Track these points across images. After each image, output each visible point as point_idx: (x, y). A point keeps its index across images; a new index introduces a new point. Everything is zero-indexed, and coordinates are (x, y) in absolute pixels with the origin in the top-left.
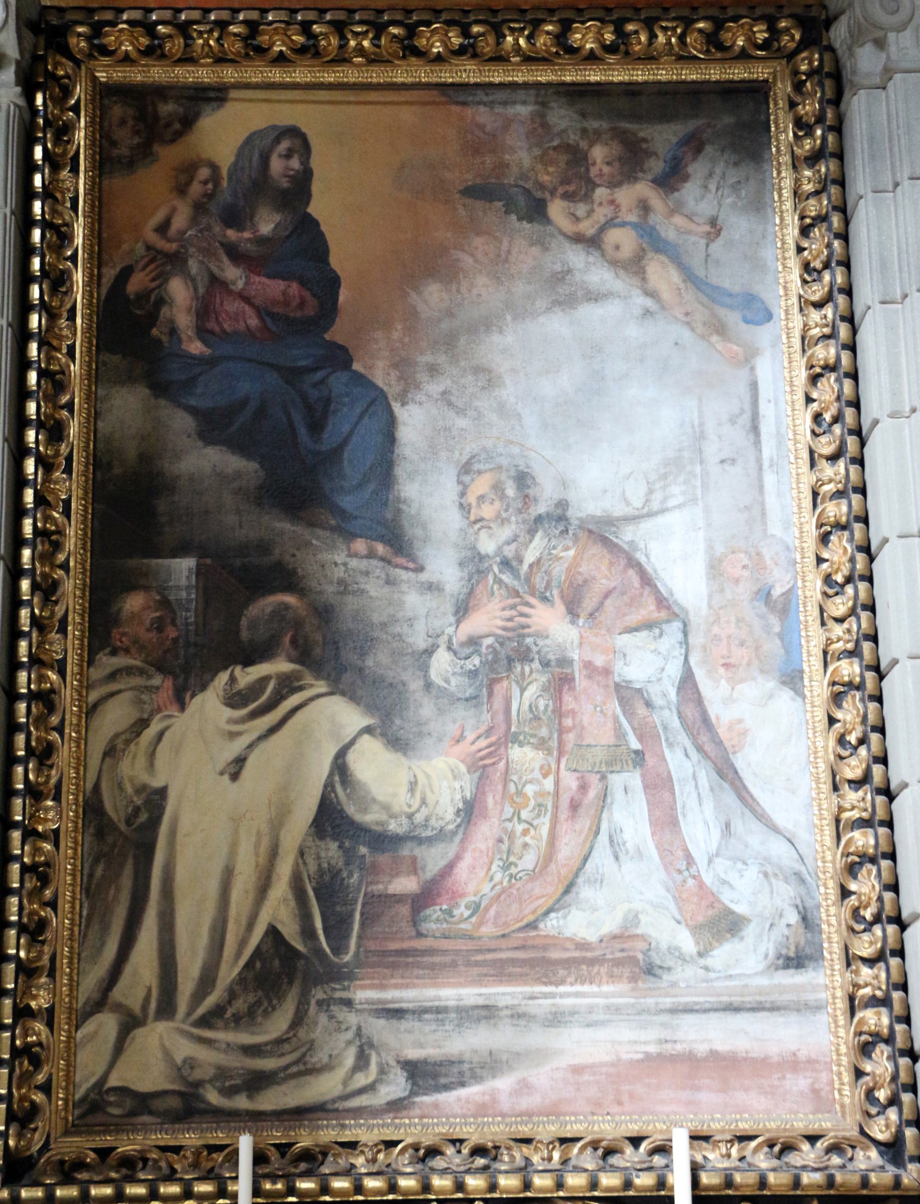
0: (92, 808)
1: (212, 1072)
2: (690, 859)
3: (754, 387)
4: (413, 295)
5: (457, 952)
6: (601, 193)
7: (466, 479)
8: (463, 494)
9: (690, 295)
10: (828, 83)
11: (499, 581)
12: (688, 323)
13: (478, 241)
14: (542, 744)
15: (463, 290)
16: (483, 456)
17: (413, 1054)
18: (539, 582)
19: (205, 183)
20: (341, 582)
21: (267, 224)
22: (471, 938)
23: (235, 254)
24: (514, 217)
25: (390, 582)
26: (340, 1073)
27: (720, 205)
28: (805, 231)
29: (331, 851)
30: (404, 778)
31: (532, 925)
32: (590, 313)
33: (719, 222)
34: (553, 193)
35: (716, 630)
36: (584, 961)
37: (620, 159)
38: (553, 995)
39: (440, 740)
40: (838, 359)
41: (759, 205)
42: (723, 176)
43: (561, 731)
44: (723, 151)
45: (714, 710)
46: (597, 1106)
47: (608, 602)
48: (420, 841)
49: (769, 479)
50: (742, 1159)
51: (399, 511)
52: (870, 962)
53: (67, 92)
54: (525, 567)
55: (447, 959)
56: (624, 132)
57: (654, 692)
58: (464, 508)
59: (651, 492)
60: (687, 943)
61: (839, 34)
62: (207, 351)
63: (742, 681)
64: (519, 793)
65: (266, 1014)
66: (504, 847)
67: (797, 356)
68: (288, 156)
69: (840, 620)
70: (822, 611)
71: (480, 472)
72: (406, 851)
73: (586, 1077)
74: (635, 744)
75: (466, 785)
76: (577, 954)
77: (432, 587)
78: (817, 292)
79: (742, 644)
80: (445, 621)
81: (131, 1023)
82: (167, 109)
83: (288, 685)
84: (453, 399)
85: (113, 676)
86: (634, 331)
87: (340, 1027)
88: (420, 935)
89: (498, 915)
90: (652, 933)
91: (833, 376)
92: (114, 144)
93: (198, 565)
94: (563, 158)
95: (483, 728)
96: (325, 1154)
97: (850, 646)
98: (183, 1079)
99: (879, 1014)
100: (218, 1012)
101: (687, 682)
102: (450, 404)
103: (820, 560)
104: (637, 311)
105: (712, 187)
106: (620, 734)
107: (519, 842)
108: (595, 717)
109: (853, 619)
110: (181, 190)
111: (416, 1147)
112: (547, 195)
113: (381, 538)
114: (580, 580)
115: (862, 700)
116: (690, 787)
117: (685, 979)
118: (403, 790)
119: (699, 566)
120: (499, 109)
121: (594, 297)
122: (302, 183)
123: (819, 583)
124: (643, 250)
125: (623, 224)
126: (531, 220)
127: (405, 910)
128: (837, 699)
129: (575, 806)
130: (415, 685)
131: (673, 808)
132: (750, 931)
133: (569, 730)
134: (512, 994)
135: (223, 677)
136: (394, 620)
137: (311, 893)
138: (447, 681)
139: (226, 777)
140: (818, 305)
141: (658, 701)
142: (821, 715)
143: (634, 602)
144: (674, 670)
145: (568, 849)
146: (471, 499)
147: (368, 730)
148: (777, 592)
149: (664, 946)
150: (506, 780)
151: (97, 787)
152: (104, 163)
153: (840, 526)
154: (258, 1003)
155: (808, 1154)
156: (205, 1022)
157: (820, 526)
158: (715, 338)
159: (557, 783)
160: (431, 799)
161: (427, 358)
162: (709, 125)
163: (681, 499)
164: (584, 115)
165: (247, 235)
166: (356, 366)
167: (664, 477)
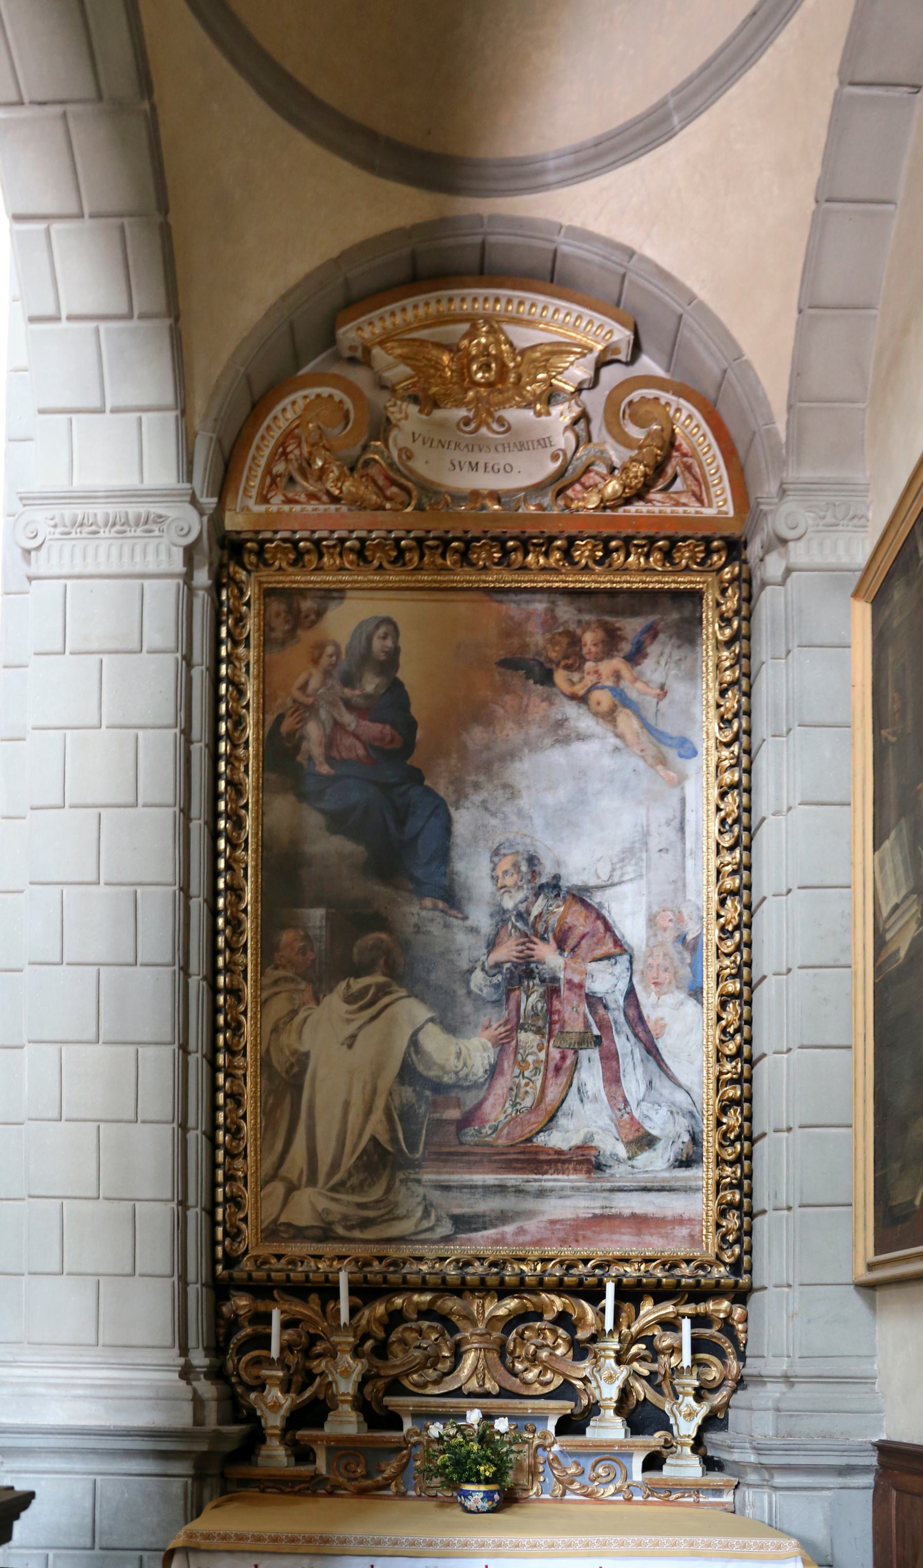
0: (265, 1063)
1: (339, 1217)
2: (626, 1102)
3: (683, 801)
4: (464, 734)
5: (484, 1154)
6: (589, 665)
7: (496, 859)
8: (493, 870)
9: (645, 737)
10: (744, 586)
11: (514, 927)
12: (643, 757)
13: (508, 698)
14: (539, 1031)
15: (497, 731)
16: (507, 844)
17: (457, 1211)
18: (540, 928)
19: (331, 656)
20: (416, 926)
21: (371, 684)
22: (492, 1146)
23: (349, 705)
24: (531, 681)
25: (446, 926)
26: (414, 1220)
27: (667, 675)
28: (723, 693)
29: (408, 1093)
30: (453, 1050)
31: (529, 1140)
32: (579, 748)
33: (666, 688)
34: (558, 665)
35: (650, 961)
36: (559, 1161)
37: (603, 642)
38: (540, 1180)
39: (476, 1027)
40: (740, 780)
41: (692, 676)
42: (670, 656)
43: (552, 1023)
44: (671, 637)
45: (645, 1013)
46: (564, 1242)
47: (584, 942)
48: (462, 1088)
49: (689, 863)
50: (647, 1272)
51: (452, 880)
52: (731, 1164)
53: (242, 593)
54: (532, 918)
55: (478, 1158)
56: (606, 623)
57: (610, 1000)
58: (495, 879)
59: (613, 870)
60: (622, 1151)
61: (753, 551)
62: (332, 772)
63: (664, 994)
64: (524, 1060)
65: (370, 1186)
66: (514, 1093)
67: (712, 779)
68: (385, 637)
69: (728, 955)
70: (718, 949)
71: (505, 855)
72: (453, 1094)
73: (558, 1226)
74: (596, 1032)
75: (490, 1055)
76: (555, 1157)
77: (473, 930)
78: (728, 735)
79: (666, 970)
80: (480, 952)
81: (291, 1188)
82: (307, 605)
83: (383, 990)
84: (489, 806)
85: (276, 982)
86: (607, 762)
87: (413, 1195)
88: (461, 1144)
89: (508, 1133)
90: (601, 1145)
91: (736, 792)
92: (272, 629)
93: (327, 914)
94: (565, 641)
95: (502, 1021)
96: (405, 1264)
97: (733, 971)
98: (323, 1220)
99: (734, 1194)
100: (342, 1183)
101: (631, 993)
102: (486, 809)
103: (719, 916)
104: (610, 748)
105: (663, 662)
106: (587, 1026)
107: (523, 1090)
108: (573, 1014)
109: (738, 954)
110: (316, 661)
111: (457, 1261)
112: (554, 666)
113: (442, 898)
114: (566, 927)
115: (740, 1005)
116: (629, 1059)
117: (620, 1173)
118: (453, 1058)
119: (642, 921)
120: (523, 606)
121: (582, 737)
122: (393, 656)
123: (717, 932)
124: (615, 706)
125: (603, 688)
126: (542, 684)
127: (453, 1129)
128: (723, 1005)
129: (557, 1069)
130: (461, 992)
131: (618, 1071)
132: (660, 1146)
133: (556, 1022)
134: (516, 1179)
135: (343, 985)
136: (448, 950)
137: (396, 1117)
138: (481, 990)
139: (345, 1047)
140: (728, 745)
141: (612, 1005)
142: (713, 1015)
143: (600, 942)
144: (623, 986)
145: (553, 1094)
146: (499, 872)
147: (432, 1020)
148: (690, 937)
149: (608, 1153)
150: (516, 1052)
151: (268, 1051)
152: (267, 642)
153: (734, 893)
154: (365, 1179)
155: (685, 1269)
156: (334, 1189)
157: (720, 894)
158: (660, 767)
159: (547, 1055)
160: (469, 1063)
161: (472, 778)
162: (662, 620)
163: (632, 875)
164: (580, 611)
165: (357, 692)
166: (427, 783)
167: (622, 860)
